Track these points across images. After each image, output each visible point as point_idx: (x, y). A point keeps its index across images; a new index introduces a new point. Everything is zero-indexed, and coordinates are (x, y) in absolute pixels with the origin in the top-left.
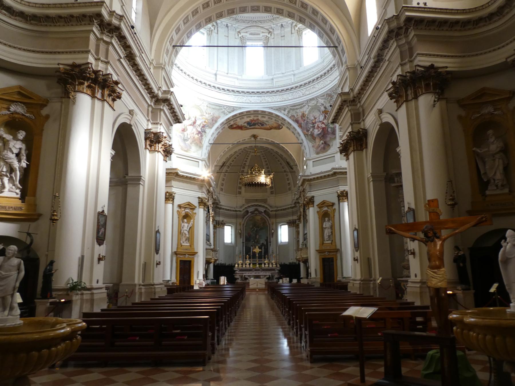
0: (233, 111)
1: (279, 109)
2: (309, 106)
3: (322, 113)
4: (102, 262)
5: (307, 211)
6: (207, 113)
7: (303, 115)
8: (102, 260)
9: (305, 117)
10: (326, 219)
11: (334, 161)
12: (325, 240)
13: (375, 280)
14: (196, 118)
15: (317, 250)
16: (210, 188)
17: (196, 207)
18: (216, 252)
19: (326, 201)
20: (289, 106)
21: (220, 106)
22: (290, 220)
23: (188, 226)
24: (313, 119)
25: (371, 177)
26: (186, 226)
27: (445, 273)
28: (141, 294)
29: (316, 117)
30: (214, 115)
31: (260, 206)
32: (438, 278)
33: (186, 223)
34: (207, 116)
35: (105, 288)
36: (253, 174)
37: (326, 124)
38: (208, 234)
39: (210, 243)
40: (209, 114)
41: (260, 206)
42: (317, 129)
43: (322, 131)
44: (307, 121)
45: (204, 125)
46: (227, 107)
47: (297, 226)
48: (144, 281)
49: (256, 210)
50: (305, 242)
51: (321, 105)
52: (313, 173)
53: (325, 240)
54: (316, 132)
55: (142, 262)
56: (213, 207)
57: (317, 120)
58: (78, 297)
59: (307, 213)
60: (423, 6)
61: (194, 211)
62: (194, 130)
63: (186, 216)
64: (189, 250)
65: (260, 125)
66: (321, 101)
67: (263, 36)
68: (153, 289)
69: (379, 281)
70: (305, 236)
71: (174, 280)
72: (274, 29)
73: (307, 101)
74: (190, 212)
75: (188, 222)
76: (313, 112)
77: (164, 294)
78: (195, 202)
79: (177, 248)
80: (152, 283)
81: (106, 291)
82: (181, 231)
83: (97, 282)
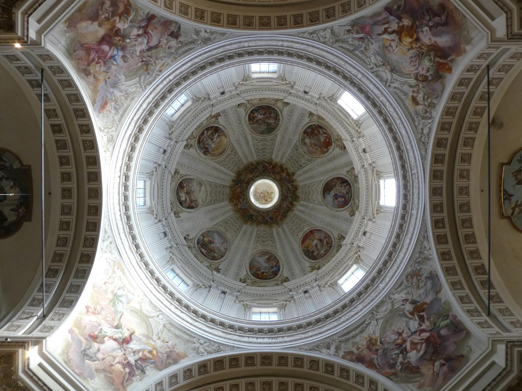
3: (410, 316)
9: (376, 345)
14: (133, 333)
20: (335, 337)
21: (190, 336)
24: (396, 337)
30: (174, 348)
34: (159, 343)
40: (163, 341)
45: (145, 356)
46: (205, 342)
51: (402, 303)
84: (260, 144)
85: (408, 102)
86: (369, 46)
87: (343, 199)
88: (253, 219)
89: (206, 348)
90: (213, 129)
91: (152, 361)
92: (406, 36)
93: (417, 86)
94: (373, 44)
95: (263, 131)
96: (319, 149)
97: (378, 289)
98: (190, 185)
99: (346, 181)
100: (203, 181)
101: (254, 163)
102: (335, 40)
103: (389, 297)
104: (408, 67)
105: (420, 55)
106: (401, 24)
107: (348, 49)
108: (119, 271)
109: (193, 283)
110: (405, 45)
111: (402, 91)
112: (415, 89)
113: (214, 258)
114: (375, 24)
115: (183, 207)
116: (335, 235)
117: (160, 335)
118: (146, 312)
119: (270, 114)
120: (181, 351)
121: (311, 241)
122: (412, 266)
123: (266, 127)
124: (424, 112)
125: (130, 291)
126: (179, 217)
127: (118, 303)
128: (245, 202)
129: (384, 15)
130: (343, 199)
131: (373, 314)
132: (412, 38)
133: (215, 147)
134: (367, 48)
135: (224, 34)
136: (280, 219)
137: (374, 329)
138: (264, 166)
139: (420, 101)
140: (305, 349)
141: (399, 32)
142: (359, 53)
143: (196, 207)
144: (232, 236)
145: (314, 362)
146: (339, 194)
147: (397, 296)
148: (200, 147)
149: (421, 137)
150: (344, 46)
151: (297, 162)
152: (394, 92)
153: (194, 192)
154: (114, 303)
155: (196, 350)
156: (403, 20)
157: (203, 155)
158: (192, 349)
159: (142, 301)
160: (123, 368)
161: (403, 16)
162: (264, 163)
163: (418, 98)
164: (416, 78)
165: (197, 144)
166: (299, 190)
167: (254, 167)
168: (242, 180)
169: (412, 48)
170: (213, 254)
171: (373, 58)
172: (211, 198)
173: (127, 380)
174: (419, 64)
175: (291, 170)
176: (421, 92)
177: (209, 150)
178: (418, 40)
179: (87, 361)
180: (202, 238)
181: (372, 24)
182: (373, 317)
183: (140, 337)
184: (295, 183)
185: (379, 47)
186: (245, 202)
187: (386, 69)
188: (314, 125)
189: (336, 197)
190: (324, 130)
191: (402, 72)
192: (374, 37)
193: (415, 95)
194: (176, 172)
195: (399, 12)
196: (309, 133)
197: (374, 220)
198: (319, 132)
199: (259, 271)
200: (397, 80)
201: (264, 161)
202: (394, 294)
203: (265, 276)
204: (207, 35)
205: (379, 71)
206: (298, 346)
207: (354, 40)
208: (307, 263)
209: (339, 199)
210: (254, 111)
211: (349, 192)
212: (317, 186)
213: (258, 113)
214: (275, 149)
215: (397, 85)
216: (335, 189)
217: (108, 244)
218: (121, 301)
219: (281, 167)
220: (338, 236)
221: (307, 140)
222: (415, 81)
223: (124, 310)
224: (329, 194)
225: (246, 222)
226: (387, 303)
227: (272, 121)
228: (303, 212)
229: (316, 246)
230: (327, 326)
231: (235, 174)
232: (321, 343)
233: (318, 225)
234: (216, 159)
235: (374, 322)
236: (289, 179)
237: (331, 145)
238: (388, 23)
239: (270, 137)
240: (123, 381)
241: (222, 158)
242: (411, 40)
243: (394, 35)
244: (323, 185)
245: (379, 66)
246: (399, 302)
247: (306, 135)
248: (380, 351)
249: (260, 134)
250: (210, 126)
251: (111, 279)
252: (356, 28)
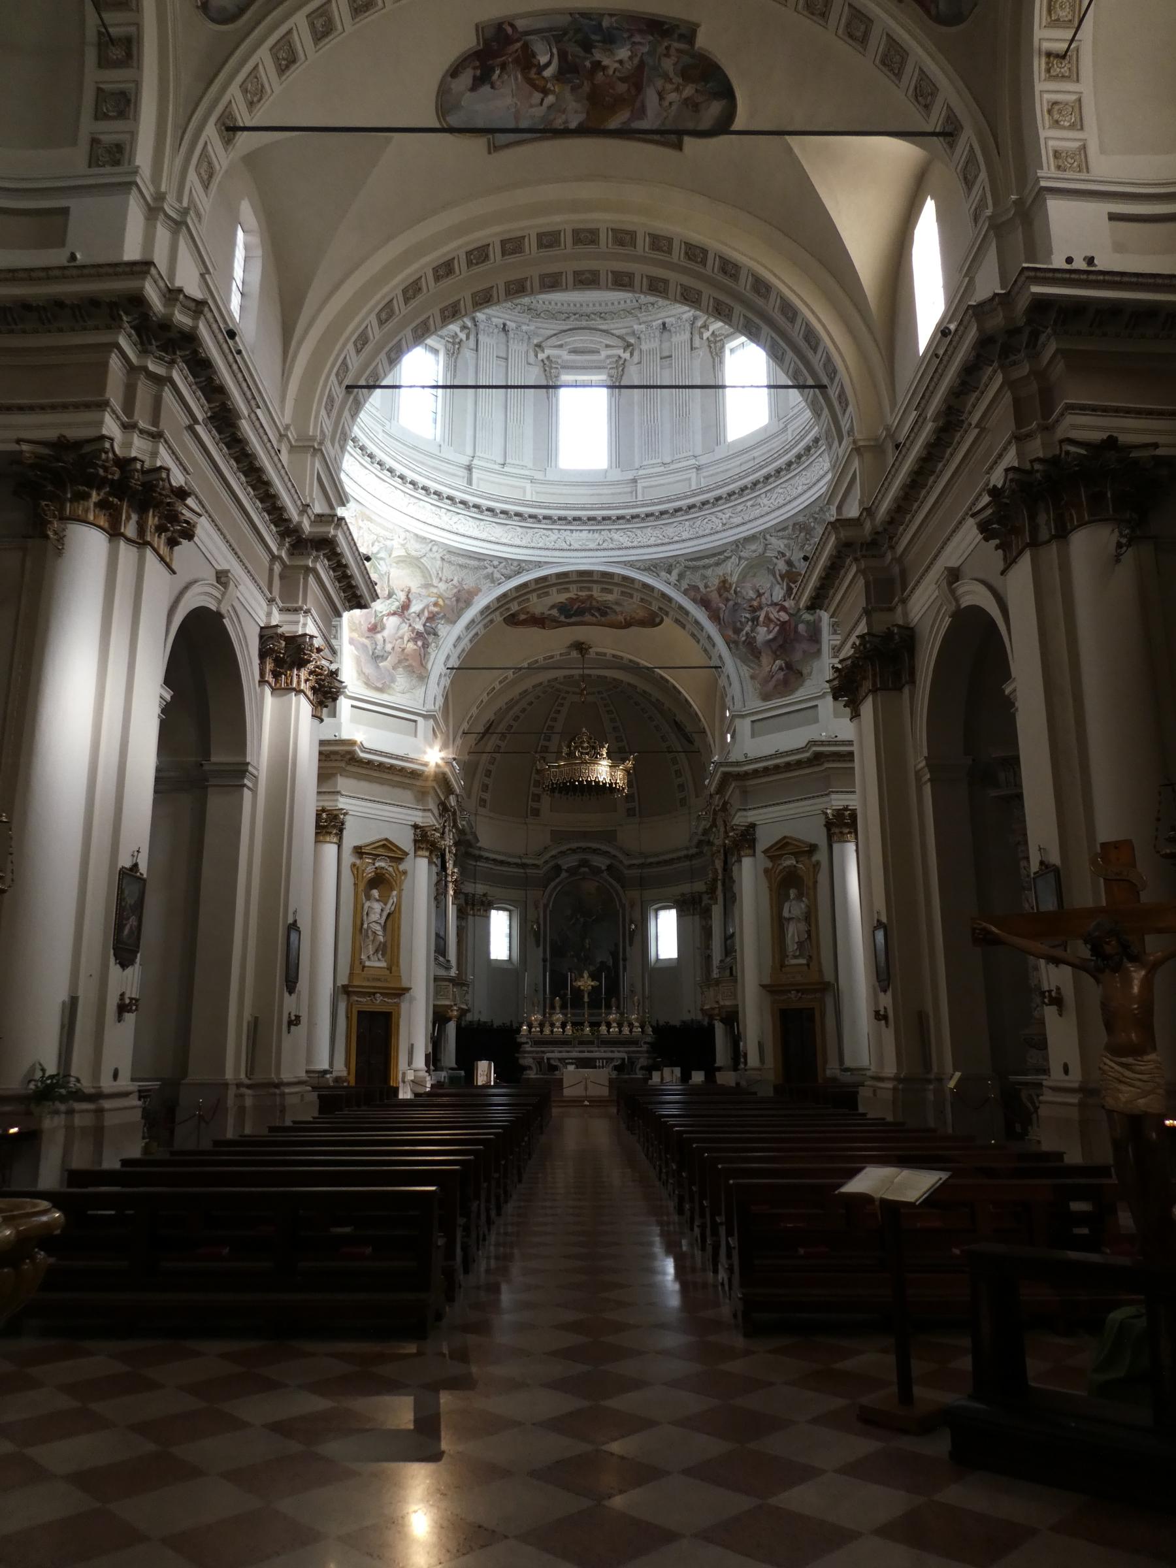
0: (519, 573)
1: (652, 567)
2: (740, 558)
3: (779, 578)
4: (130, 1018)
5: (735, 868)
6: (441, 579)
7: (724, 586)
8: (130, 1011)
9: (728, 591)
10: (793, 893)
11: (816, 720)
12: (787, 956)
13: (940, 1080)
15: (763, 986)
16: (447, 797)
17: (407, 854)
18: (465, 988)
19: (791, 838)
21: (479, 559)
22: (683, 895)
23: (382, 910)
24: (754, 596)
25: (926, 770)
26: (376, 910)
27: (1157, 1068)
28: (242, 1110)
29: (761, 591)
31: (595, 851)
32: (1138, 1083)
33: (377, 901)
34: (442, 586)
35: (136, 1095)
36: (576, 758)
37: (791, 611)
38: (442, 934)
39: (448, 961)
40: (446, 582)
41: (595, 851)
43: (779, 632)
44: (736, 604)
45: (432, 612)
46: (500, 563)
47: (706, 913)
48: (252, 1074)
49: (584, 863)
50: (728, 959)
52: (751, 755)
53: (787, 956)
54: (763, 634)
55: (247, 1016)
56: (455, 855)
57: (763, 599)
58: (60, 1120)
59: (735, 875)
60: (1083, 266)
61: (402, 867)
62: (405, 627)
63: (379, 881)
64: (386, 981)
65: (596, 614)
66: (778, 544)
67: (608, 357)
68: (278, 1099)
69: (952, 1084)
70: (729, 942)
71: (340, 1069)
72: (642, 336)
73: (736, 543)
74: (391, 869)
75: (383, 899)
77: (309, 1113)
78: (405, 840)
79: (351, 974)
80: (276, 1081)
81: (140, 1103)
82: (362, 924)
83: (115, 1076)
179: (381, 664)
183: (418, 591)
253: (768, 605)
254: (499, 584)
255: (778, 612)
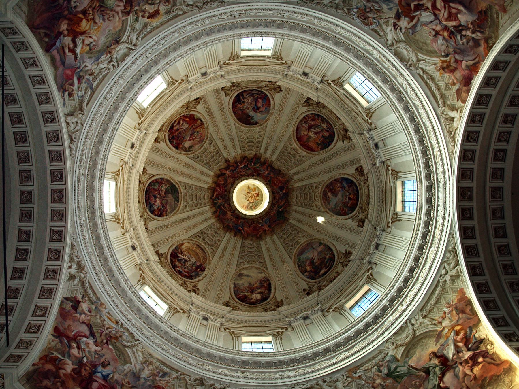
29: (434, 33)
30: (452, 305)
34: (446, 323)
40: (444, 318)
42: (456, 19)
45: (462, 339)
46: (445, 268)
57: (438, 28)
66: (390, 34)
73: (408, 67)
76: (425, 43)
84: (191, 203)
85: (155, 22)
86: (88, 71)
87: (260, 100)
88: (282, 211)
89: (451, 267)
90: (174, 260)
91: (468, 330)
92: (79, 26)
93: (138, 12)
94: (86, 66)
95: (175, 199)
96: (198, 130)
97: (379, 59)
98: (242, 288)
99: (238, 96)
100: (237, 272)
101: (214, 209)
102: (80, 112)
103: (390, 46)
104: (116, 22)
105: (102, 9)
106: (66, 32)
107: (90, 95)
108: (358, 371)
109: (367, 283)
110: (90, 27)
111: (142, 30)
112: (140, 14)
113: (332, 259)
114: (63, 63)
115: (269, 297)
116: (303, 110)
117: (436, 322)
118: (408, 339)
119: (155, 190)
120: (455, 297)
121: (310, 140)
122: (353, 18)
123: (170, 195)
124: (167, 4)
125: (383, 359)
126: (282, 301)
127: (399, 372)
128: (261, 221)
129: (55, 53)
130: (260, 100)
131: (410, 65)
132: (82, 19)
133: (195, 257)
134: (90, 72)
135: (72, 246)
136: (283, 177)
137: (430, 65)
138: (217, 197)
139: (154, 8)
140: (453, 148)
141: (75, 34)
142: (96, 82)
143: (269, 280)
144: (303, 237)
145: (468, 136)
146: (253, 106)
147: (390, 37)
148: (196, 276)
149: (197, 6)
150: (86, 101)
151: (213, 157)
152: (142, 39)
153: (250, 283)
154: (398, 377)
155: (454, 278)
156: (61, 30)
157: (205, 272)
158: (453, 284)
159: (395, 344)
160: (478, 365)
161: (57, 31)
162: (214, 198)
163: (151, 11)
164: (128, 13)
165: (192, 279)
166: (247, 154)
167: (218, 210)
168: (234, 225)
169: (93, 19)
170: (326, 260)
171: (102, 66)
172: (258, 263)
173: (493, 359)
174: (112, 10)
175: (223, 164)
176: (144, 8)
177: (198, 264)
178: (84, 12)
180: (307, 274)
181: (64, 66)
182: (414, 66)
183: (438, 345)
184: (239, 159)
185: (89, 58)
186: (261, 221)
187: (115, 49)
188: (168, 136)
189: (256, 109)
190: (175, 124)
191: (120, 30)
192: (79, 64)
193: (147, 15)
194: (227, 304)
195: (53, 35)
196: (178, 142)
197: (289, 63)
198: (177, 130)
199: (347, 203)
200: (129, 36)
201: (211, 198)
202: (387, 40)
203: (353, 197)
204: (74, 266)
205: (116, 58)
206: (449, 156)
207: (80, 89)
208: (338, 145)
209: (259, 105)
210: (152, 209)
211: (250, 93)
212: (242, 132)
213: (153, 205)
214: (196, 183)
215: (134, 37)
216: (246, 110)
217: (326, 385)
218: (396, 368)
219: (218, 176)
220: (305, 106)
221: (187, 144)
222: (131, 15)
223: (406, 365)
224: (252, 118)
225: (286, 220)
226: (398, 49)
227: (163, 188)
228: (275, 149)
229: (316, 133)
230: (424, 121)
231: (228, 234)
232: (446, 128)
233: (291, 130)
234: (209, 256)
235: (422, 64)
236: (233, 166)
237: (192, 115)
238: (63, 48)
239: (182, 190)
240: (494, 364)
241: (208, 249)
242: (84, 20)
243: (77, 40)
244: (241, 125)
245: (112, 58)
246: (397, 33)
247: (181, 146)
248: (458, 57)
249: (178, 202)
250: (170, 263)
251: (368, 381)
252: (67, 86)
253: (440, 23)
254: (461, 272)
255: (439, 10)
